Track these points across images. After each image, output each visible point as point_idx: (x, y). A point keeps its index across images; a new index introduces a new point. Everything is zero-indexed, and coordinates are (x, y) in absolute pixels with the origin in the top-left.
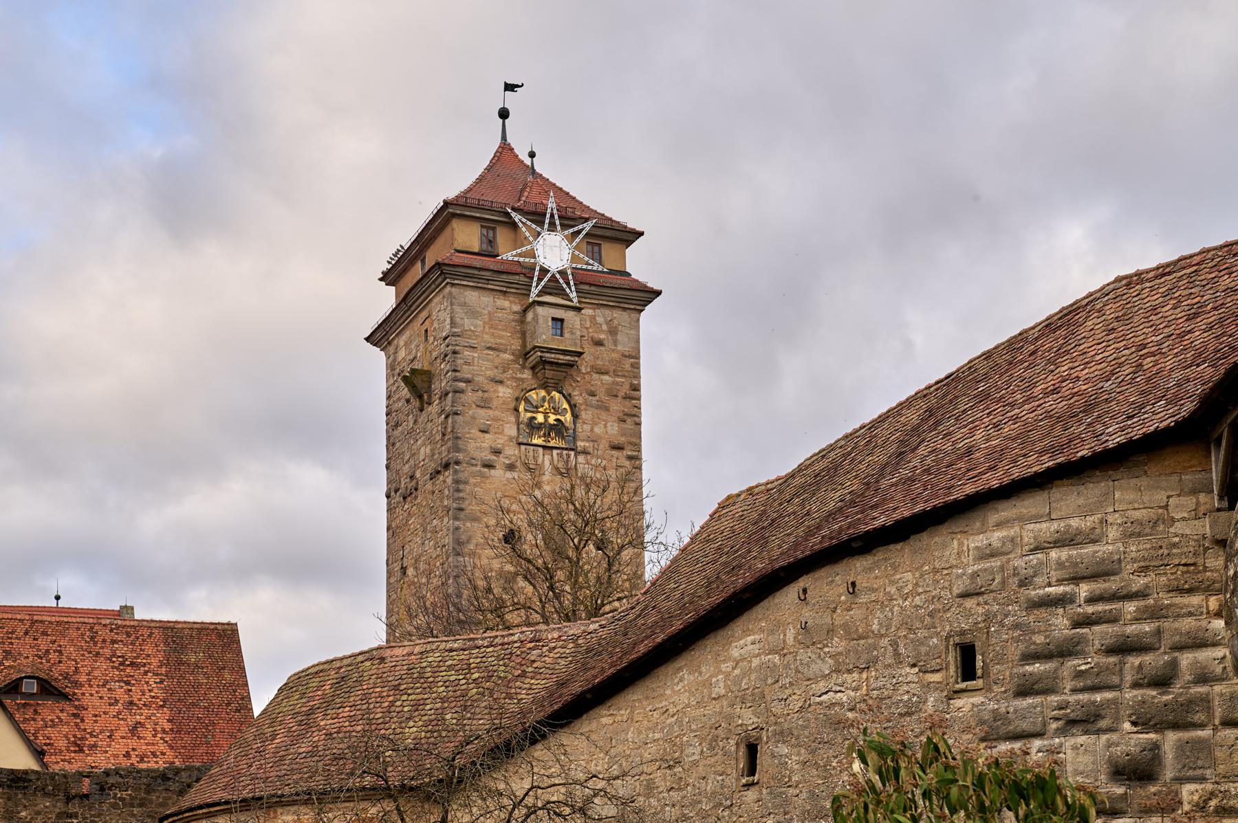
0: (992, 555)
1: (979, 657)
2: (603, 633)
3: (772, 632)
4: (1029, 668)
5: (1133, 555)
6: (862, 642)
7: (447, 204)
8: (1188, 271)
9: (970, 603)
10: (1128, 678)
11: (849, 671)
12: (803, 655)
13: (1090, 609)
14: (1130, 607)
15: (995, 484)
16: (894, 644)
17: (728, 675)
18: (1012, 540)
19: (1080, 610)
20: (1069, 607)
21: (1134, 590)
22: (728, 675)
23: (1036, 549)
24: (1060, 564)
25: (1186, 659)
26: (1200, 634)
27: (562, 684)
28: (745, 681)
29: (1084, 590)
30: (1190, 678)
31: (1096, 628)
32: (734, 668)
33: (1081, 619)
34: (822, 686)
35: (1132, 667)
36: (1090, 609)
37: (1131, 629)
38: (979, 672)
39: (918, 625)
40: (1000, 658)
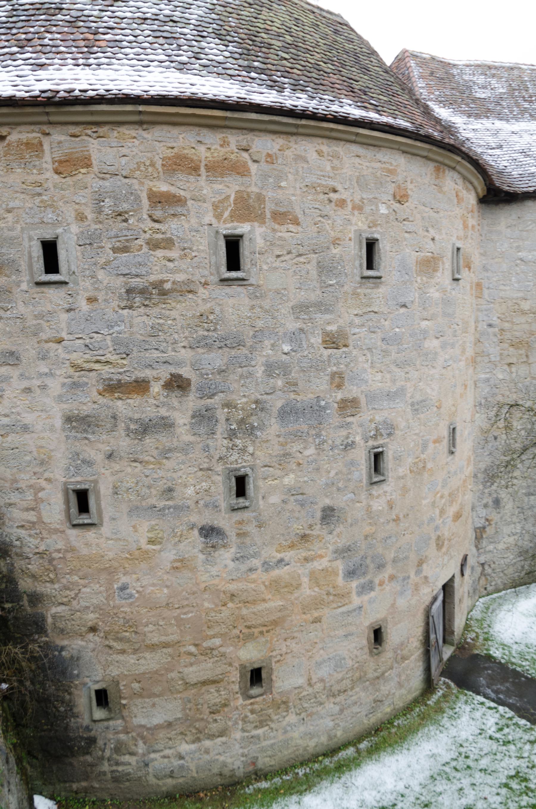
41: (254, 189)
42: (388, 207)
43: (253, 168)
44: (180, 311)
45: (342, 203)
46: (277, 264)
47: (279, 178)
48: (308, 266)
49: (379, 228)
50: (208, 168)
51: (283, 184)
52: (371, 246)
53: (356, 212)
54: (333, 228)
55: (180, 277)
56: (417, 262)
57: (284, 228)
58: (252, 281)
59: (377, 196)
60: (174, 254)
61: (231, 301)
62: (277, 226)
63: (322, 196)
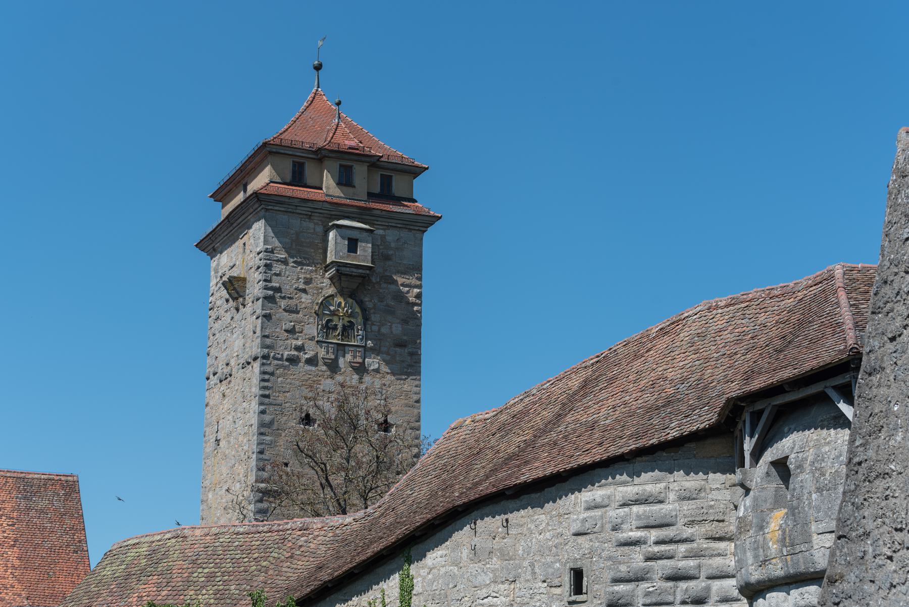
0: (596, 507)
1: (585, 579)
2: (356, 526)
3: (453, 550)
4: (616, 588)
5: (685, 512)
6: (511, 562)
7: (265, 144)
8: (743, 305)
9: (581, 539)
10: (679, 598)
11: (502, 583)
12: (474, 568)
13: (656, 549)
14: (682, 548)
15: (597, 458)
16: (532, 565)
17: (424, 578)
18: (609, 497)
19: (650, 549)
20: (643, 546)
21: (685, 537)
22: (424, 578)
23: (624, 505)
24: (639, 517)
25: (716, 585)
26: (725, 569)
27: (320, 568)
28: (435, 584)
29: (654, 535)
30: (718, 599)
31: (660, 562)
32: (429, 573)
33: (650, 555)
34: (483, 592)
35: (682, 590)
36: (656, 549)
37: (682, 564)
38: (584, 591)
39: (547, 552)
40: (597, 581)
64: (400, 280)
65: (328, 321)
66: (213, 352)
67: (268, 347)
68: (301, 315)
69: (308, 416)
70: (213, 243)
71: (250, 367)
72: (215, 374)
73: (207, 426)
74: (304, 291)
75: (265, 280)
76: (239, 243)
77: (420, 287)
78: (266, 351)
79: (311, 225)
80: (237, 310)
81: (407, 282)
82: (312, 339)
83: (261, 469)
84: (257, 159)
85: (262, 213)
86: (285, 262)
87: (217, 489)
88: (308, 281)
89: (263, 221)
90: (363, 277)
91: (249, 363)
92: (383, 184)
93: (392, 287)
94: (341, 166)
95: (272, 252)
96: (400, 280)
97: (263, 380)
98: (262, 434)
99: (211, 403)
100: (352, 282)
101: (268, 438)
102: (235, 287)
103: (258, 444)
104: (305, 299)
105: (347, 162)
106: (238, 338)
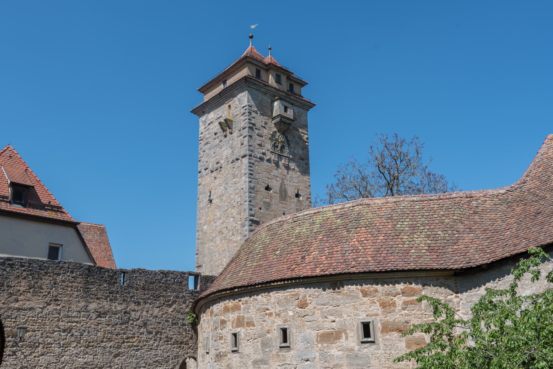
41: (242, 314)
42: (293, 312)
43: (242, 306)
44: (224, 363)
45: (271, 314)
46: (249, 343)
47: (248, 309)
48: (258, 344)
49: (288, 323)
50: (232, 309)
51: (250, 311)
52: (284, 331)
53: (277, 317)
54: (267, 326)
55: (224, 350)
56: (318, 336)
57: (249, 328)
58: (240, 351)
59: (288, 307)
60: (222, 341)
61: (235, 359)
62: (248, 328)
63: (263, 313)
64: (300, 130)
65: (275, 143)
66: (203, 159)
67: (251, 151)
68: (263, 138)
69: (268, 186)
70: (201, 110)
71: (239, 161)
72: (205, 170)
73: (200, 194)
74: (264, 127)
75: (249, 119)
76: (226, 106)
77: (307, 134)
78: (251, 152)
79: (266, 98)
80: (225, 136)
81: (303, 131)
82: (268, 150)
83: (251, 210)
84: (238, 65)
85: (247, 88)
86: (256, 113)
87: (212, 223)
88: (266, 123)
89: (247, 92)
90: (290, 124)
91: (237, 159)
92: (291, 88)
93: (297, 132)
94: (276, 74)
95: (251, 107)
96: (300, 130)
97: (250, 166)
98: (250, 192)
99: (203, 183)
100: (286, 126)
101: (253, 195)
102: (226, 125)
103: (249, 197)
104: (265, 132)
105: (281, 72)
106: (226, 149)
